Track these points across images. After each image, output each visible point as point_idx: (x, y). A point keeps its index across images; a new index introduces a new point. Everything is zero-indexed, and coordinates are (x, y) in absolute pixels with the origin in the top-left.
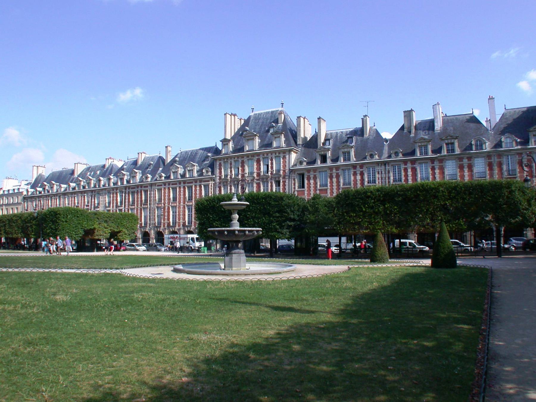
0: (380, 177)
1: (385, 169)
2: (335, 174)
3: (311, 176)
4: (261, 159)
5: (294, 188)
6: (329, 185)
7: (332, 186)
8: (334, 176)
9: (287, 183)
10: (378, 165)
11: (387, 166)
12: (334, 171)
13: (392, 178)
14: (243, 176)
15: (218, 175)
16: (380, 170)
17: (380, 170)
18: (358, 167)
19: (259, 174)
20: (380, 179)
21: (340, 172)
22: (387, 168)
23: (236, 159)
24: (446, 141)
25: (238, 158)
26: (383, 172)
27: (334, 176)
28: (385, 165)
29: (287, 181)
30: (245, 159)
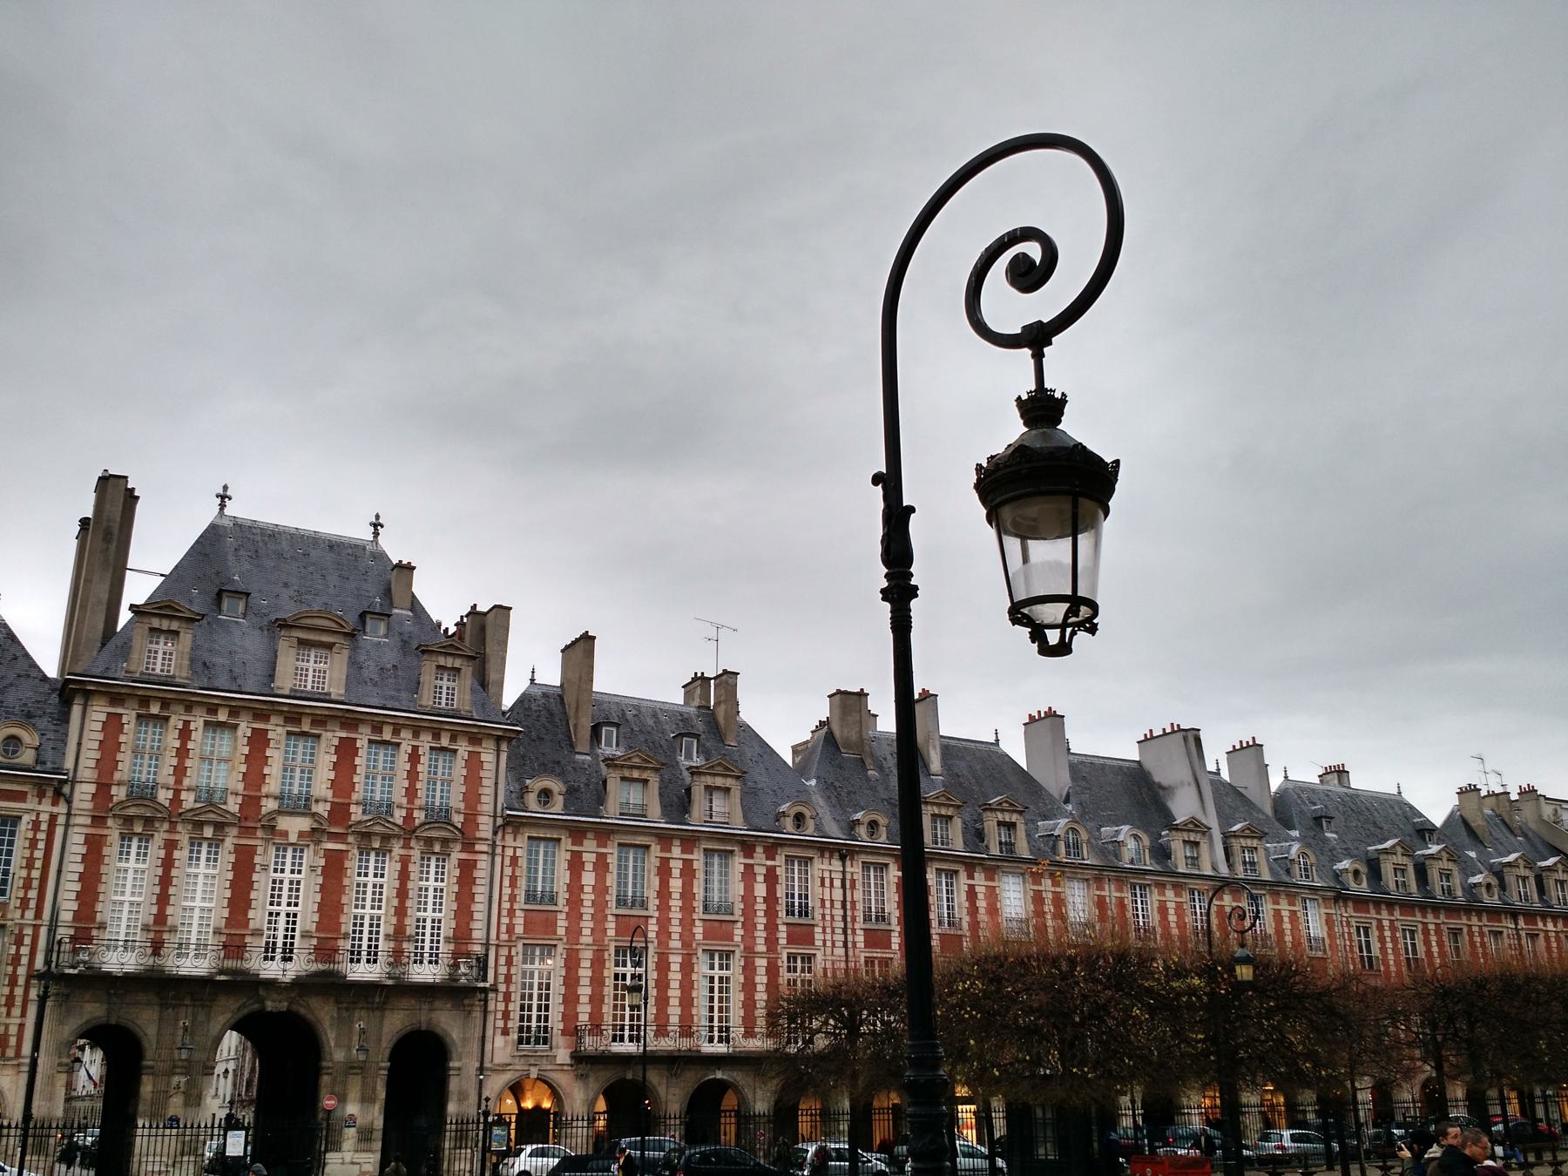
0: (827, 897)
1: (844, 872)
2: (679, 864)
3: (585, 857)
4: (362, 742)
5: (512, 898)
6: (653, 903)
7: (664, 907)
8: (676, 873)
9: (481, 873)
10: (822, 856)
11: (848, 863)
12: (676, 851)
13: (860, 906)
14: (251, 802)
15: (87, 771)
16: (826, 875)
17: (826, 875)
18: (759, 850)
19: (340, 812)
20: (828, 904)
21: (698, 858)
22: (848, 869)
23: (222, 716)
24: (1000, 816)
25: (234, 712)
26: (837, 883)
27: (676, 873)
28: (843, 858)
29: (483, 863)
30: (276, 730)
